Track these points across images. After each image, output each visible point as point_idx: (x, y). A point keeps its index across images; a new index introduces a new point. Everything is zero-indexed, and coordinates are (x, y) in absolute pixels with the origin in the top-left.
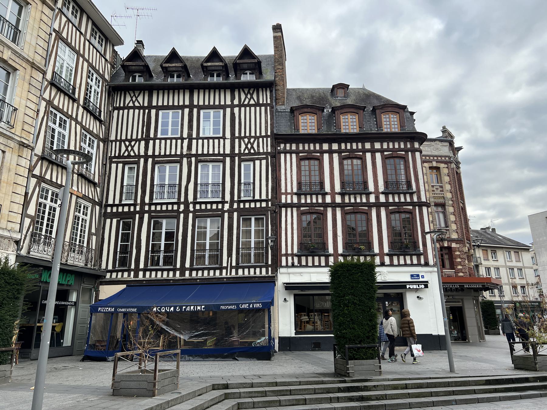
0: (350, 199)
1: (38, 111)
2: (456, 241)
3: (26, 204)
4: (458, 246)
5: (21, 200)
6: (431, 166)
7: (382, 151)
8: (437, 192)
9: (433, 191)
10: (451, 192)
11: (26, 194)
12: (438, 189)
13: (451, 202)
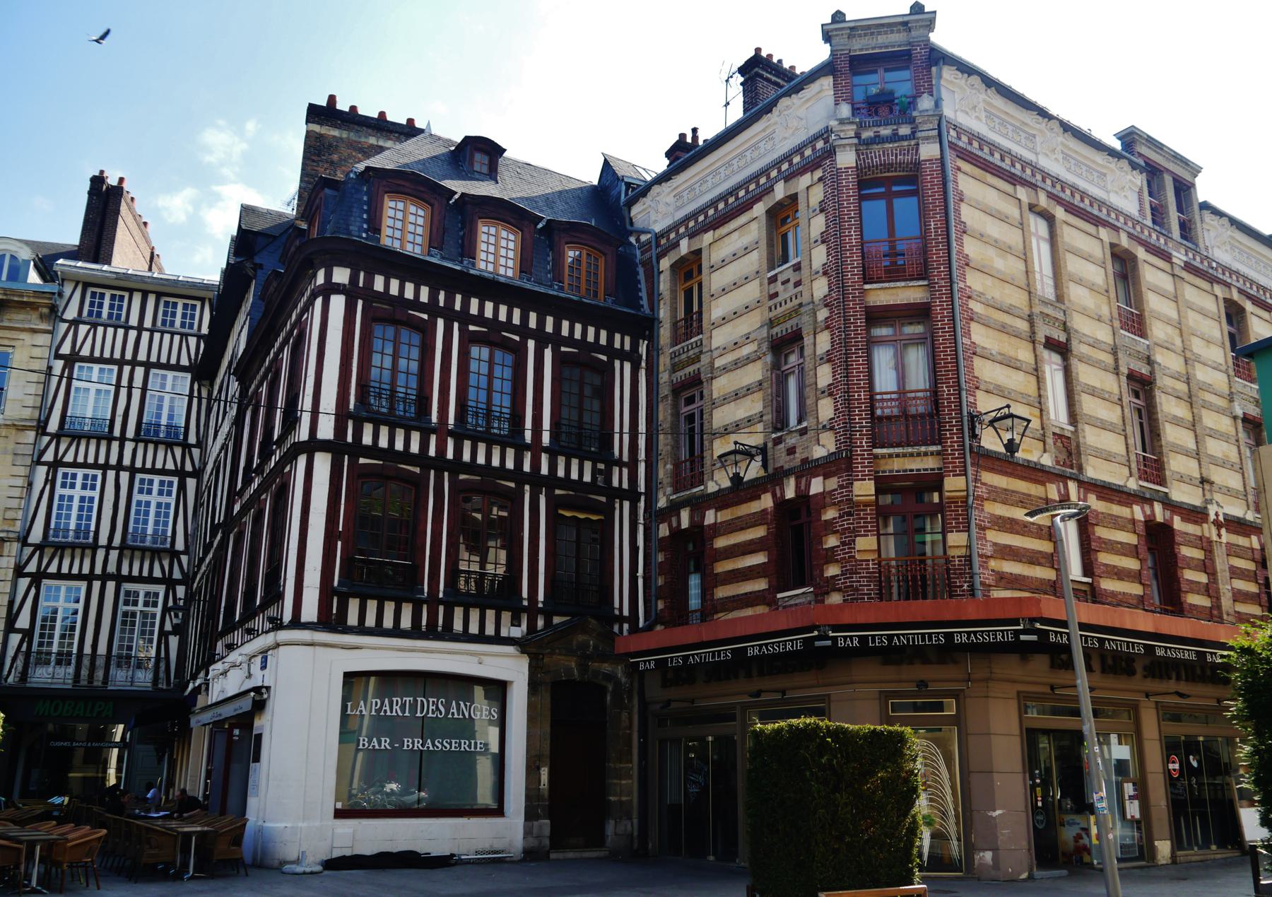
1: (30, 484)
2: (826, 467)
3: (11, 618)
4: (833, 483)
6: (771, 204)
8: (787, 295)
9: (776, 295)
10: (825, 273)
11: (11, 603)
12: (788, 281)
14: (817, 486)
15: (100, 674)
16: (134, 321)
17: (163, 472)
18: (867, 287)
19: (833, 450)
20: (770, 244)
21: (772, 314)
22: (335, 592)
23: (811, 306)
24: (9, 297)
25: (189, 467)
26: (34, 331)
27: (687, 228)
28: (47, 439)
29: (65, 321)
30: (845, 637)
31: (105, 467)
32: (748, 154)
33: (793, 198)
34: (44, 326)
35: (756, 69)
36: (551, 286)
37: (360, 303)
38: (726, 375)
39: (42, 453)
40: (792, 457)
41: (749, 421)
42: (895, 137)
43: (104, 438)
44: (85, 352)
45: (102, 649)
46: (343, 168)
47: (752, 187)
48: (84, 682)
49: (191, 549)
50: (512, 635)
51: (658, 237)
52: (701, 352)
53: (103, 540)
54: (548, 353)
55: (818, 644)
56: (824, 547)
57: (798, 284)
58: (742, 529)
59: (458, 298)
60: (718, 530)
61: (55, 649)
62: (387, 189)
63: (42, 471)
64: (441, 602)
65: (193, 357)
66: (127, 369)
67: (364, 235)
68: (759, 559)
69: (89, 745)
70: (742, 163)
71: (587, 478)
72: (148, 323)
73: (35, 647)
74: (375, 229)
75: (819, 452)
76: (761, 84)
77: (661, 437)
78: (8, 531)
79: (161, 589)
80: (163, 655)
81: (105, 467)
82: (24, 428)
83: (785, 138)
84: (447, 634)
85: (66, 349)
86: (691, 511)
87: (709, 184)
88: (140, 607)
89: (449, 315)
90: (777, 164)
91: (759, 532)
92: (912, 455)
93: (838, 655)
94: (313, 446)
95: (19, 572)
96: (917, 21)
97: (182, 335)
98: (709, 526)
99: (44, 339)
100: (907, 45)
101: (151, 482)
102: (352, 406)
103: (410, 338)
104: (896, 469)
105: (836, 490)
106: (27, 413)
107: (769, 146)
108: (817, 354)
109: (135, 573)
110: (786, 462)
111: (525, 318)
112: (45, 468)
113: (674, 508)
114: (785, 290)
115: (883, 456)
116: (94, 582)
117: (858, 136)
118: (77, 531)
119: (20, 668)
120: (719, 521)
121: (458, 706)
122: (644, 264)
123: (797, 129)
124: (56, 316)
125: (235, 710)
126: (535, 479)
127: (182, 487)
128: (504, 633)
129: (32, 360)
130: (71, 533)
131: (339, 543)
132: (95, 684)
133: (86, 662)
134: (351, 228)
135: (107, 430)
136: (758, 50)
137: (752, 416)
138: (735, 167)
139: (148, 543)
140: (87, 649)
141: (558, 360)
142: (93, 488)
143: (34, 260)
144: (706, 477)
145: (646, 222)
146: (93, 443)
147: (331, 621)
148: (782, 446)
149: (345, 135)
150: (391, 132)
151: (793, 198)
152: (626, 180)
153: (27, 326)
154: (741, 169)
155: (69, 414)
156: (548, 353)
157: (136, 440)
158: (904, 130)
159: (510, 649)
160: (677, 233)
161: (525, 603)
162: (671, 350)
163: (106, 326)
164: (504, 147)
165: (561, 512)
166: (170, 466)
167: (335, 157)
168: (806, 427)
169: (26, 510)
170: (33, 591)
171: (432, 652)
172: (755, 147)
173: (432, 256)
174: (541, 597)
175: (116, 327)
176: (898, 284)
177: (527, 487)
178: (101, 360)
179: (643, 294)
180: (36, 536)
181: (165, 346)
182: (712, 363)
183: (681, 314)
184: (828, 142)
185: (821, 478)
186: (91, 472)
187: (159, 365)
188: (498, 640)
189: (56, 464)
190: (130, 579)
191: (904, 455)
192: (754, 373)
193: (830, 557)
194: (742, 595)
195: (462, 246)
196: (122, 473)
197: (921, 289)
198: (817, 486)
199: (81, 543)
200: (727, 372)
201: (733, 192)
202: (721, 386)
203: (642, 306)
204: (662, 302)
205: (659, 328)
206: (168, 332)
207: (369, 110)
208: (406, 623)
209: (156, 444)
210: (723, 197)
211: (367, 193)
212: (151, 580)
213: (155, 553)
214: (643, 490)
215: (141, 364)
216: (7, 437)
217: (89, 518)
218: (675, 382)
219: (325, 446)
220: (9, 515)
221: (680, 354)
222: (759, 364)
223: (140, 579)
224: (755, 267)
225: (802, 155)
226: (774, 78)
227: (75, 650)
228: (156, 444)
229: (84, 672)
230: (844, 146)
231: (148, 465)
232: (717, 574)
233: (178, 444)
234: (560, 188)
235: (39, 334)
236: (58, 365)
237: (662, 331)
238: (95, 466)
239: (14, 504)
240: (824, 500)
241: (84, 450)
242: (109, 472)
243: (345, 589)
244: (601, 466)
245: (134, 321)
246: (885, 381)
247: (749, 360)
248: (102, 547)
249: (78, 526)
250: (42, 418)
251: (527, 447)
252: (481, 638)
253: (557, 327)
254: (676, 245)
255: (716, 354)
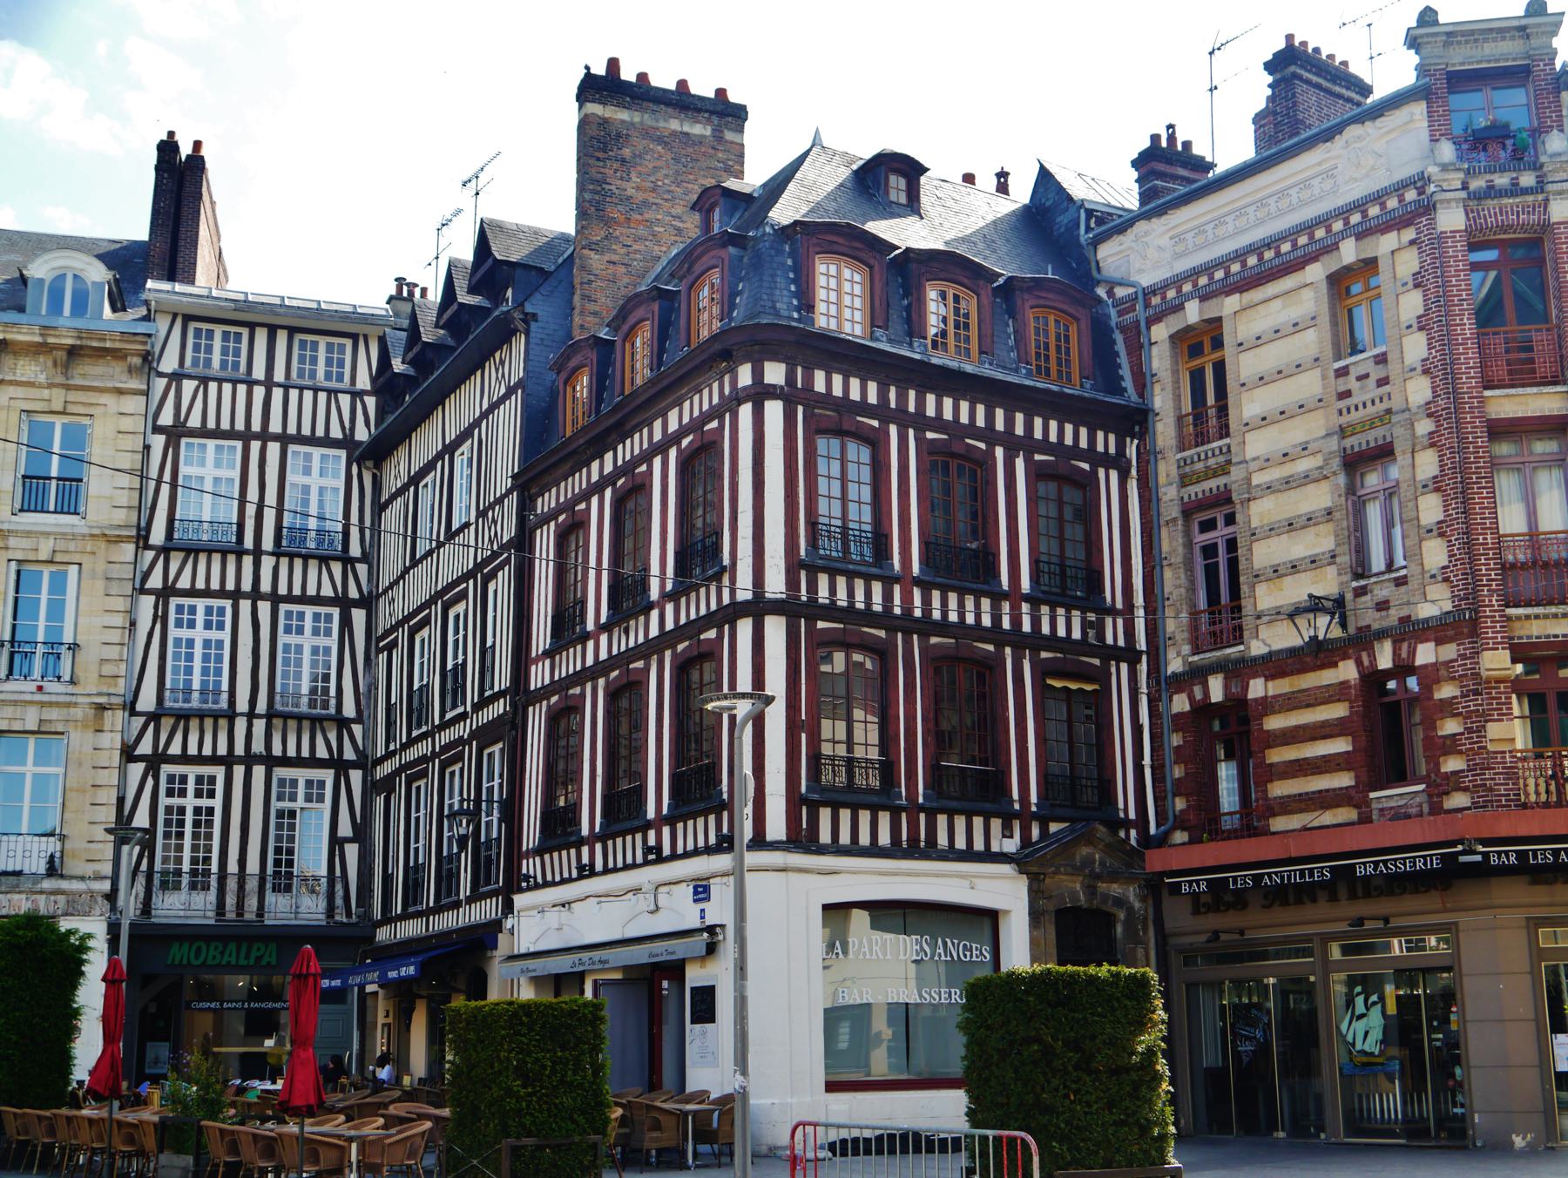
0: (833, 590)
1: (133, 624)
2: (1438, 630)
4: (1450, 651)
5: (109, 815)
6: (1334, 267)
7: (675, 439)
8: (1367, 397)
9: (1347, 394)
10: (1426, 372)
11: (121, 801)
12: (1367, 376)
13: (1424, 427)
14: (1425, 654)
15: (252, 903)
16: (259, 373)
17: (318, 600)
18: (1487, 393)
19: (1448, 606)
20: (1334, 323)
21: (1345, 419)
22: (804, 800)
23: (1406, 415)
24: (84, 342)
25: (353, 593)
26: (120, 392)
27: (1195, 285)
28: (150, 555)
29: (161, 375)
30: (1499, 853)
31: (236, 595)
32: (1293, 192)
33: (1369, 265)
34: (136, 384)
35: (1293, 68)
36: (1017, 370)
37: (800, 409)
38: (1273, 497)
39: (146, 575)
40: (1384, 613)
41: (1313, 562)
42: (1515, 190)
43: (232, 552)
44: (194, 422)
45: (253, 866)
46: (639, 168)
47: (1303, 240)
48: (231, 915)
49: (366, 714)
50: (1005, 850)
51: (1149, 292)
52: (1229, 462)
53: (242, 705)
54: (1020, 464)
55: (1462, 859)
56: (1440, 733)
57: (1383, 382)
58: (1308, 706)
59: (912, 394)
60: (1267, 706)
61: (186, 867)
62: (818, 249)
63: (148, 602)
64: (921, 808)
65: (347, 425)
66: (255, 446)
67: (796, 315)
68: (1340, 746)
69: (246, 1005)
70: (1284, 204)
71: (1076, 634)
72: (279, 376)
73: (158, 866)
74: (808, 306)
75: (1426, 611)
76: (1300, 88)
77: (1168, 574)
78: (109, 695)
79: (328, 775)
80: (338, 872)
81: (236, 595)
82: (119, 540)
83: (1356, 180)
84: (930, 851)
85: (166, 419)
86: (1225, 678)
87: (1230, 227)
88: (301, 802)
89: (903, 419)
90: (1344, 212)
91: (1338, 711)
92: (1555, 616)
93: (1484, 872)
94: (759, 608)
95: (128, 754)
96: (1539, 25)
97: (329, 391)
98: (1256, 700)
99: (135, 404)
100: (1524, 59)
101: (301, 616)
102: (803, 552)
103: (859, 454)
104: (1535, 634)
105: (1456, 660)
106: (120, 517)
107: (1328, 185)
108: (1418, 478)
109: (292, 752)
110: (1375, 620)
111: (990, 418)
112: (152, 598)
113: (1197, 674)
114: (1362, 388)
115: (1519, 618)
116: (235, 767)
117: (1465, 187)
118: (203, 692)
119: (141, 895)
120: (1270, 693)
121: (945, 944)
122: (1123, 329)
123: (1373, 168)
124: (150, 368)
125: (651, 955)
126: (1016, 639)
127: (346, 622)
128: (995, 848)
129: (120, 436)
130: (196, 695)
131: (804, 736)
132: (247, 916)
133: (232, 884)
134: (778, 305)
135: (234, 540)
136: (1290, 38)
137: (1317, 555)
138: (1273, 208)
139: (304, 708)
140: (233, 867)
141: (1037, 474)
142: (221, 627)
143: (109, 282)
144: (1246, 634)
145: (1123, 269)
146: (217, 558)
147: (801, 839)
148: (1368, 597)
149: (637, 117)
150: (699, 110)
151: (1369, 265)
152: (1088, 206)
153: (110, 385)
154: (1281, 213)
155: (177, 517)
156: (1020, 464)
157: (277, 554)
158: (1528, 179)
159: (1006, 869)
160: (1179, 290)
161: (1017, 806)
162: (1179, 456)
163: (220, 381)
164: (927, 166)
165: (1049, 682)
166: (327, 591)
167: (627, 152)
168: (1405, 576)
169: (129, 662)
170: (150, 782)
171: (918, 875)
172: (1305, 184)
173: (877, 340)
174: (1034, 798)
175: (235, 382)
176: (1529, 390)
177: (1008, 650)
178: (217, 434)
179: (1125, 371)
180: (147, 702)
181: (306, 412)
182: (1248, 480)
183: (1187, 407)
184: (1424, 193)
185: (1431, 645)
186: (216, 603)
187: (300, 439)
188: (988, 856)
189: (167, 591)
190: (285, 761)
191: (1546, 617)
192: (1320, 497)
193: (1450, 746)
194: (1313, 793)
195: (909, 320)
196: (259, 603)
197: (1557, 397)
198: (1425, 654)
199: (210, 710)
200: (1274, 492)
201: (1272, 243)
202: (1261, 512)
203: (1125, 390)
204: (1157, 388)
205: (1154, 423)
206: (309, 388)
207: (663, 80)
208: (884, 839)
209: (306, 558)
210: (1257, 249)
211: (792, 254)
212: (313, 762)
213: (316, 722)
214: (1144, 648)
215: (276, 438)
216: (94, 553)
217: (218, 672)
218: (1186, 499)
219: (777, 607)
220: (108, 669)
221: (1192, 462)
222: (1324, 487)
223: (298, 762)
224: (1313, 351)
225: (1383, 205)
226: (1315, 79)
227: (214, 868)
228: (306, 558)
229: (231, 901)
230: (1449, 201)
231: (297, 591)
232: (1271, 765)
233: (336, 559)
234: (990, 218)
235: (129, 397)
236: (158, 442)
237: (1160, 427)
238: (222, 593)
239: (113, 653)
240: (1431, 676)
241: (209, 572)
242: (241, 601)
243: (816, 797)
244: (1092, 617)
245: (259, 373)
246: (1512, 520)
247: (1307, 479)
248: (242, 714)
249: (204, 683)
250: (143, 524)
251: (1005, 596)
252: (969, 855)
253: (1029, 427)
254: (1179, 308)
255: (1253, 466)
